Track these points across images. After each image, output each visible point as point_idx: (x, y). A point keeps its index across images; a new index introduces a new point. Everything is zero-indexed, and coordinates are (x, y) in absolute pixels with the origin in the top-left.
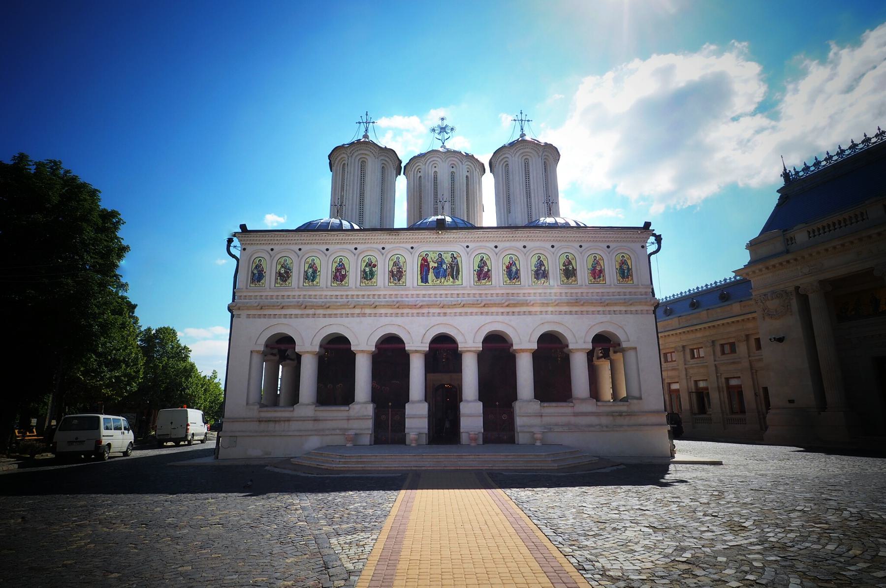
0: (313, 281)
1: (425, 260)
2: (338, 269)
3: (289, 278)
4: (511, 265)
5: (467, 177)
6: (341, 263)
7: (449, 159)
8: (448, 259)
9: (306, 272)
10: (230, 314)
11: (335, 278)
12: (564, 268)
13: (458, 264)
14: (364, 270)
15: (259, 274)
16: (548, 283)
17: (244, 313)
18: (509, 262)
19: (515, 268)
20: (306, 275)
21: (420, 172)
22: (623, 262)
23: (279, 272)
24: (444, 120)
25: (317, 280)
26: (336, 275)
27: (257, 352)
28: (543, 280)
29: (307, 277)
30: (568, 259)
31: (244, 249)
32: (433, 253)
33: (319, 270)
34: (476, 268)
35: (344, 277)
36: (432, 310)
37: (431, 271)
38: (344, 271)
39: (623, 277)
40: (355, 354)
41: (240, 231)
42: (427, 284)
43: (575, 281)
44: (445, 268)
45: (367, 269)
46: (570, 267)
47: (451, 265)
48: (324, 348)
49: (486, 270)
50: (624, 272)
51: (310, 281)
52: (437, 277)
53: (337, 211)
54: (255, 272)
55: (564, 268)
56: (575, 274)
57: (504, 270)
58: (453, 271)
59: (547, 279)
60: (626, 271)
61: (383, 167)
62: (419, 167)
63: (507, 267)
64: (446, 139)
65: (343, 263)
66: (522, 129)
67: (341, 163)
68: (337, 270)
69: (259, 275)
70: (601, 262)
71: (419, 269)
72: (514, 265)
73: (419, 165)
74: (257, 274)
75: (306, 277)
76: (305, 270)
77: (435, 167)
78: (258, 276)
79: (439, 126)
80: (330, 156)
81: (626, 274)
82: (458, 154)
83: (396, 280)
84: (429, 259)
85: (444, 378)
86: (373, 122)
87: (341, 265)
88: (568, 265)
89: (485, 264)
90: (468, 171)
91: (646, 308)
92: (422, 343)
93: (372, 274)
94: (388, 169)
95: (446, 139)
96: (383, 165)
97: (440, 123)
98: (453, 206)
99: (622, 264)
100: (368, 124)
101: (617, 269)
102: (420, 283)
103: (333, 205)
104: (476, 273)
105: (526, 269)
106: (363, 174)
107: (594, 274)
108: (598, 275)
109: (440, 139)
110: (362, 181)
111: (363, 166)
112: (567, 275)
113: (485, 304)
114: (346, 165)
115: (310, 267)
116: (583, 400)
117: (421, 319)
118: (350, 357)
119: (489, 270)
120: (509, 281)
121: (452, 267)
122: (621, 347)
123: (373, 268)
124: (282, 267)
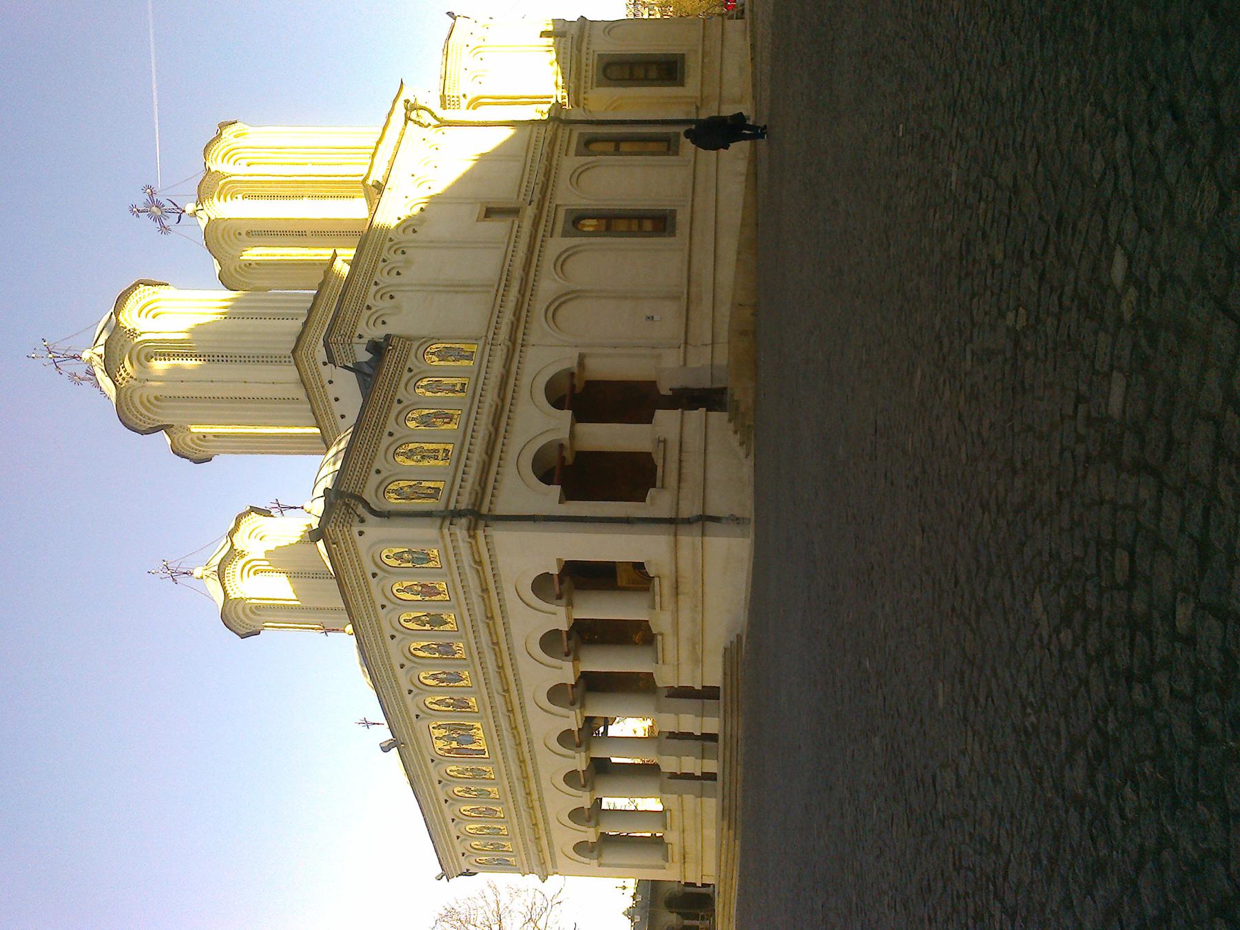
8: (442, 732)
22: (399, 557)
34: (450, 709)
37: (464, 746)
39: (429, 561)
41: (445, 877)
42: (486, 750)
46: (428, 619)
81: (421, 556)
84: (448, 747)
85: (622, 580)
88: (422, 621)
120: (465, 681)
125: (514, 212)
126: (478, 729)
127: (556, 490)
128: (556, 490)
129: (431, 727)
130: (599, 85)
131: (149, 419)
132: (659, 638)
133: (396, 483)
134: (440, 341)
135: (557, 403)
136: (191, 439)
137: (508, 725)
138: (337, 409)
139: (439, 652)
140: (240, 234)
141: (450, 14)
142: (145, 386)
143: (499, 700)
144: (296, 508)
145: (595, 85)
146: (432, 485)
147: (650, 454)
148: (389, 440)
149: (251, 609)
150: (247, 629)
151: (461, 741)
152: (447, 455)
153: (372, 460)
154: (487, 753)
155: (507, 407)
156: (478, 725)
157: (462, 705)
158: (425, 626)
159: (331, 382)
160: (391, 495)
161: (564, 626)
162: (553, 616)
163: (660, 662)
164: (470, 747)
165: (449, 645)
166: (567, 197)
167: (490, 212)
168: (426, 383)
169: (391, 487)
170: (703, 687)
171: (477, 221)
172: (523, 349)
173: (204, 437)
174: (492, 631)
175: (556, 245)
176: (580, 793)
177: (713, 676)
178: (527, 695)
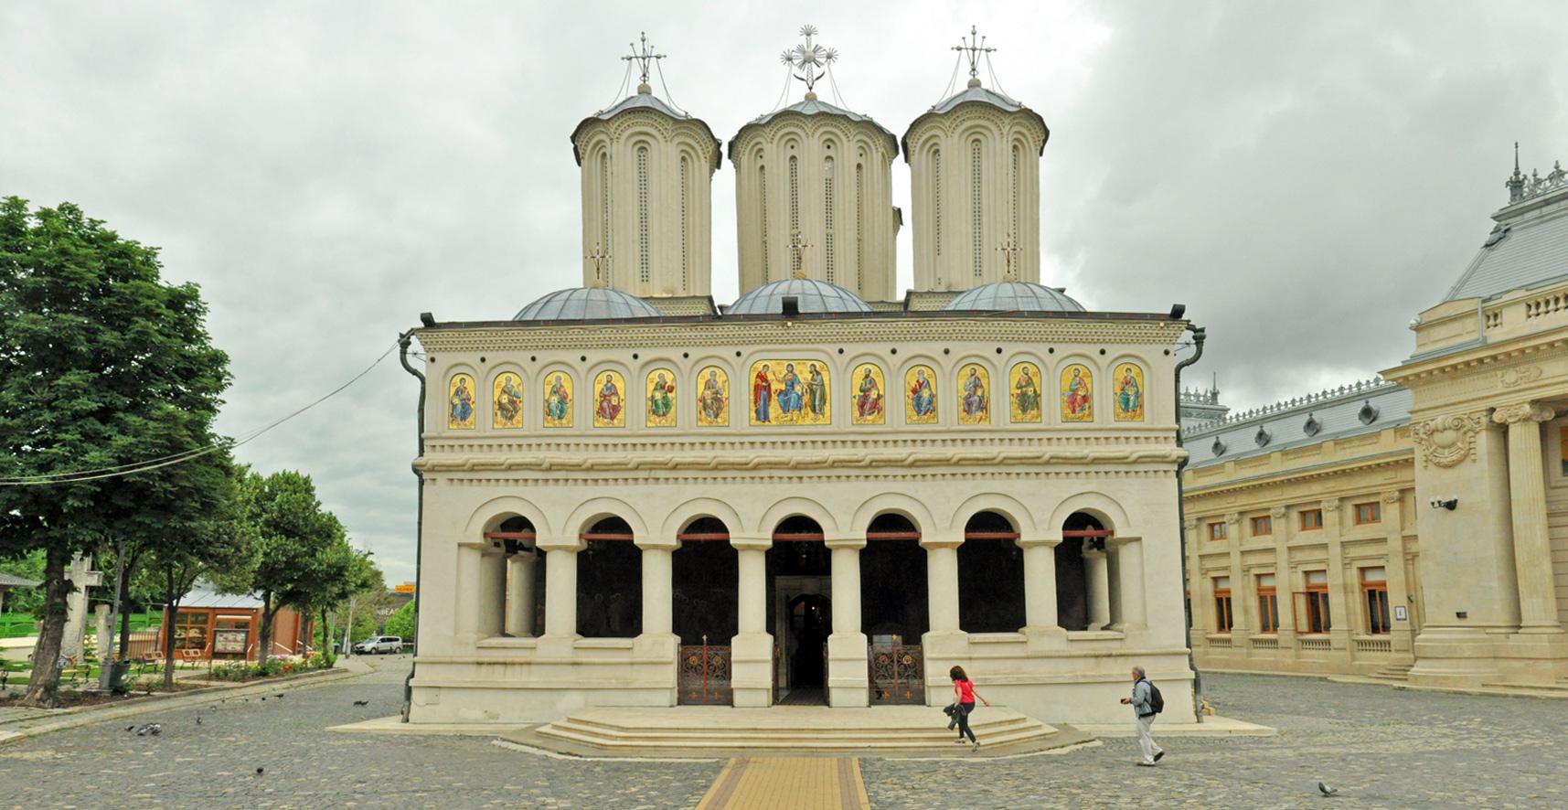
0: (560, 418)
1: (761, 377)
2: (605, 396)
3: (517, 412)
4: (920, 387)
5: (859, 166)
6: (609, 385)
7: (822, 130)
8: (804, 375)
9: (547, 401)
10: (416, 477)
11: (601, 412)
12: (1019, 391)
13: (823, 385)
14: (653, 397)
15: (463, 405)
16: (988, 420)
17: (442, 478)
18: (918, 381)
19: (929, 393)
20: (548, 407)
21: (761, 157)
23: (500, 403)
24: (812, 36)
25: (568, 416)
26: (602, 408)
28: (979, 414)
29: (550, 410)
30: (1027, 374)
31: (433, 360)
32: (778, 364)
33: (570, 397)
34: (857, 392)
35: (616, 409)
36: (776, 473)
37: (774, 396)
38: (616, 399)
39: (1126, 409)
40: (641, 551)
42: (767, 423)
43: (1037, 417)
44: (800, 393)
45: (658, 395)
46: (1030, 391)
47: (810, 386)
48: (589, 540)
49: (875, 396)
50: (1128, 399)
51: (556, 417)
53: (596, 268)
54: (456, 401)
55: (1019, 391)
56: (1037, 403)
57: (908, 396)
58: (816, 399)
60: (1132, 398)
61: (683, 159)
62: (759, 146)
63: (914, 391)
64: (818, 79)
65: (613, 385)
66: (974, 70)
67: (598, 152)
68: (603, 396)
69: (463, 408)
70: (1087, 381)
71: (752, 397)
72: (925, 387)
73: (757, 144)
74: (459, 407)
75: (549, 412)
76: (546, 398)
77: (792, 147)
78: (462, 411)
79: (801, 49)
80: (574, 138)
81: (1131, 404)
82: (840, 119)
83: (710, 416)
84: (770, 377)
86: (658, 57)
87: (610, 388)
88: (1025, 386)
89: (873, 384)
90: (861, 155)
91: (1166, 467)
92: (759, 531)
93: (667, 404)
94: (693, 161)
95: (818, 79)
96: (684, 154)
97: (803, 40)
98: (831, 231)
99: (1127, 384)
100: (647, 60)
101: (1116, 394)
102: (754, 422)
103: (588, 256)
104: (856, 401)
105: (949, 395)
106: (643, 174)
108: (1080, 406)
109: (802, 79)
110: (643, 191)
111: (642, 158)
112: (1023, 406)
113: (872, 462)
114: (608, 156)
115: (555, 392)
116: (1043, 634)
117: (758, 487)
118: (631, 557)
119: (879, 397)
120: (915, 418)
121: (811, 390)
122: (1115, 537)
123: (669, 395)
124: (504, 391)
126: (816, 419)
129: (813, 362)
137: (842, 457)
139: (970, 396)
142: (1002, 137)
148: (939, 355)
150: (616, 129)
151: (787, 395)
154: (759, 423)
156: (821, 420)
157: (867, 407)
158: (1018, 388)
162: (1046, 526)
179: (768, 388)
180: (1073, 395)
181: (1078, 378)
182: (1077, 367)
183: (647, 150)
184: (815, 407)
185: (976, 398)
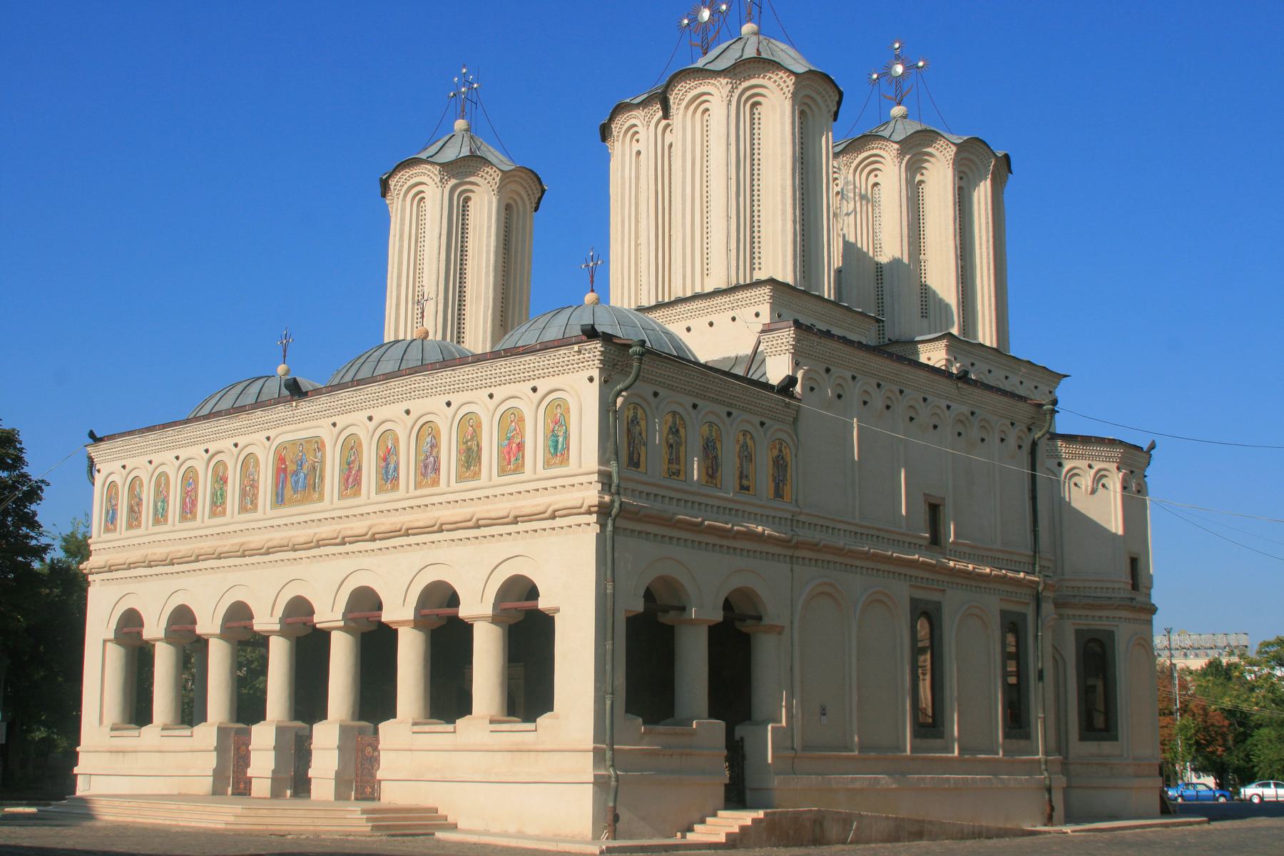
1: (282, 460)
4: (389, 453)
12: (464, 447)
27: (110, 641)
35: (194, 503)
44: (306, 472)
46: (473, 444)
50: (557, 441)
52: (295, 491)
59: (439, 475)
60: (561, 439)
63: (385, 459)
74: (111, 512)
81: (560, 446)
88: (470, 440)
99: (556, 424)
107: (509, 453)
112: (468, 463)
125: (936, 539)
127: (639, 606)
128: (639, 606)
130: (1079, 633)
131: (680, 100)
132: (450, 727)
133: (644, 415)
134: (794, 458)
135: (727, 605)
136: (635, 125)
137: (324, 536)
138: (699, 324)
139: (427, 458)
140: (876, 176)
141: (1153, 447)
143: (359, 527)
144: (592, 282)
145: (1078, 627)
146: (643, 459)
147: (673, 716)
149: (423, 192)
150: (395, 185)
152: (674, 474)
153: (670, 387)
155: (725, 542)
157: (350, 480)
159: (734, 319)
160: (632, 411)
161: (464, 612)
163: (416, 728)
164: (289, 486)
165: (437, 470)
166: (953, 603)
167: (934, 510)
168: (749, 444)
169: (640, 412)
170: (380, 781)
171: (925, 494)
172: (788, 559)
173: (637, 141)
174: (459, 525)
175: (902, 592)
176: (219, 621)
177: (394, 793)
178: (365, 561)
179: (285, 470)
180: (509, 444)
181: (513, 424)
182: (512, 411)
183: (424, 198)
184: (315, 486)
185: (432, 459)
